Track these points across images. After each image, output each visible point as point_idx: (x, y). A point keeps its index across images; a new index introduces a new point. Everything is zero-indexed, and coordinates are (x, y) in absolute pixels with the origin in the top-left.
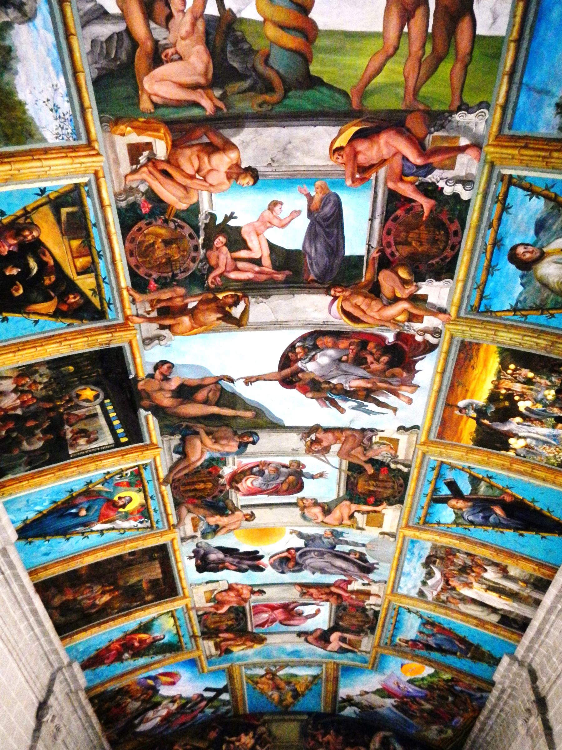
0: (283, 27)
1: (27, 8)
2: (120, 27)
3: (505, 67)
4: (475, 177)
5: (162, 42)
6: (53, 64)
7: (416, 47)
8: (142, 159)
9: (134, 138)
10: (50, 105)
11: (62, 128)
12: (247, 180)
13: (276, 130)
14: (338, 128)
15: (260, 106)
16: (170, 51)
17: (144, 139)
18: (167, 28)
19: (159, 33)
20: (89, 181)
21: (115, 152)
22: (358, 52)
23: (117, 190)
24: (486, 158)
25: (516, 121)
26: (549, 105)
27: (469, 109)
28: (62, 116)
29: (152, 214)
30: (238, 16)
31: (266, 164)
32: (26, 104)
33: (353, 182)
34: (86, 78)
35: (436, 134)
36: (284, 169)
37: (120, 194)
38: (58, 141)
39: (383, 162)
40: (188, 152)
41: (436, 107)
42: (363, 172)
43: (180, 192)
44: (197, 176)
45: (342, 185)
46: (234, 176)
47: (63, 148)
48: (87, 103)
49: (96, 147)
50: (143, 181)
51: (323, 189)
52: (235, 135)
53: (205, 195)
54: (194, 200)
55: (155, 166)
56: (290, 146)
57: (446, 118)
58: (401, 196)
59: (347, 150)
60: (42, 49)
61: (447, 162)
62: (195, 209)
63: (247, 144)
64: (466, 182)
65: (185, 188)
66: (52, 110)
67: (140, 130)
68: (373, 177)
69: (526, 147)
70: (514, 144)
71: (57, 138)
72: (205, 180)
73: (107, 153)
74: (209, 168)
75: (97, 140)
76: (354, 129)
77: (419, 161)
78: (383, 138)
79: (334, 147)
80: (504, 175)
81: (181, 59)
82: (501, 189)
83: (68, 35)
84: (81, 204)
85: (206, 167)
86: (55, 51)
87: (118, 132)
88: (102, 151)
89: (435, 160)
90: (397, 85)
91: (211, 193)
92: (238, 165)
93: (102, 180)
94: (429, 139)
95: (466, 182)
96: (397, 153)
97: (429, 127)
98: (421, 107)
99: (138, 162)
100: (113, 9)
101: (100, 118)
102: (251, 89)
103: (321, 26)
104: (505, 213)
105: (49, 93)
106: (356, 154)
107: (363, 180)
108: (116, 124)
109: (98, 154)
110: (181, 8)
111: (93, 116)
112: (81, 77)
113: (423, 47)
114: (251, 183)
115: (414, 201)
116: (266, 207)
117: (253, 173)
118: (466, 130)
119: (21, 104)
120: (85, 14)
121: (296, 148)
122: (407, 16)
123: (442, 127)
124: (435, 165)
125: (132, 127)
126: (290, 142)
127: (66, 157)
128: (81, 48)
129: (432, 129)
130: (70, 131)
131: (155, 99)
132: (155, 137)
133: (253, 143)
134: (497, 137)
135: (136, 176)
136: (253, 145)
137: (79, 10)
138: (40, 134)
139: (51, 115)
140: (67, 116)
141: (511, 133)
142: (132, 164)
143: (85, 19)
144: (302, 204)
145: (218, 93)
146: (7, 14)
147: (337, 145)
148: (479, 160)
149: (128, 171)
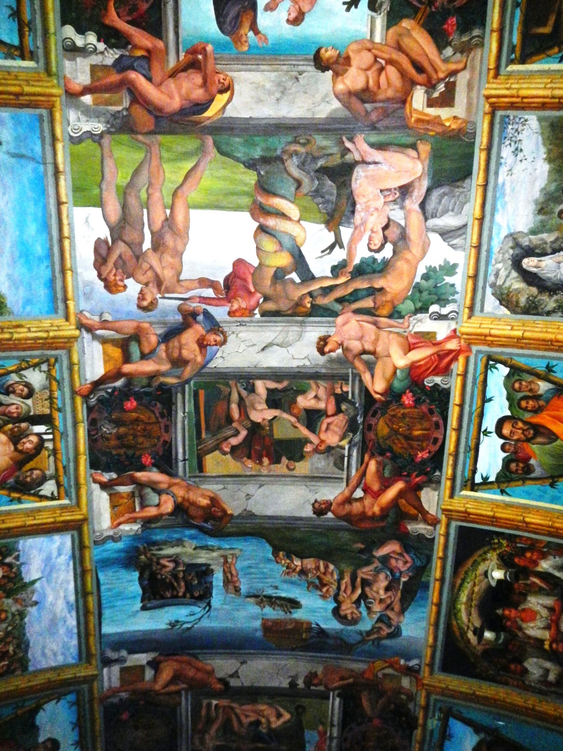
0: (283, 215)
1: (511, 244)
2: (432, 222)
3: (65, 180)
4: (64, 56)
5: (396, 207)
6: (504, 194)
7: (156, 195)
8: (441, 87)
9: (444, 113)
10: (520, 156)
11: (517, 130)
12: (328, 54)
13: (293, 115)
14: (225, 115)
15: (308, 141)
16: (391, 198)
17: (433, 112)
18: (389, 220)
19: (398, 215)
20: (507, 66)
21: (469, 98)
22: (209, 191)
23: (479, 52)
24: (58, 79)
25: (37, 124)
26: (8, 143)
27: (90, 135)
28: (513, 144)
29: (445, 14)
30: (323, 226)
31: (304, 75)
32: (545, 159)
33: (204, 49)
34: (477, 177)
35: (120, 108)
36: (285, 68)
37: (476, 45)
38: (526, 117)
39: (173, 74)
40: (390, 93)
41: (125, 137)
42: (195, 61)
43: (406, 42)
44: (383, 62)
45: (218, 45)
46: (341, 60)
47: (523, 108)
48: (483, 155)
49: (487, 106)
50: (446, 61)
51: (238, 40)
52: (336, 110)
53: (378, 39)
54: (391, 31)
55: (429, 79)
56: (278, 95)
57: (112, 126)
58: (144, 29)
59: (214, 89)
60: (510, 207)
61: (100, 74)
62: (393, 19)
63: (325, 99)
64: (72, 50)
65: (399, 48)
66: (521, 150)
67: (437, 121)
68: (182, 55)
69: (17, 95)
70: (32, 98)
71: (526, 120)
72: (376, 57)
73: (478, 98)
74: (369, 73)
75: (486, 114)
76: (209, 113)
77: (133, 75)
78: (175, 104)
79: (229, 93)
80: (31, 59)
81: (381, 191)
82: (29, 40)
83: (481, 220)
84: (526, 36)
85: (371, 74)
86: (499, 206)
87: (460, 121)
88: (482, 100)
89: (115, 78)
90: (169, 160)
91: (371, 40)
92: (337, 74)
93: (492, 66)
94: (126, 103)
95: (72, 50)
96: (158, 85)
97: (129, 115)
98: (140, 137)
99: (447, 85)
100: (435, 238)
101: (474, 138)
102: (315, 159)
103: (247, 215)
104: (14, 6)
105: (519, 167)
106: (205, 84)
107: (193, 51)
108: (460, 130)
109: (488, 97)
110: (373, 235)
111: (481, 140)
112: (481, 181)
113: (149, 196)
114: (323, 51)
115: (128, 22)
116: (307, 18)
117: (320, 63)
118: (87, 112)
119: (549, 160)
120: (460, 235)
121: (270, 93)
122: (169, 221)
123: (115, 115)
124: (114, 71)
125: (443, 125)
126: (278, 100)
127: (523, 98)
128: (473, 208)
129: (125, 113)
130: (510, 127)
131: (413, 153)
132: (421, 113)
133: (317, 99)
134: (53, 106)
135: (453, 67)
136: (318, 97)
137: (465, 239)
138: (542, 127)
139: (523, 146)
140: (508, 142)
141: (38, 111)
142: (454, 84)
143: (461, 232)
144: (264, 20)
145: (349, 157)
146: (530, 241)
147: (226, 96)
148: (65, 77)
149: (460, 75)
